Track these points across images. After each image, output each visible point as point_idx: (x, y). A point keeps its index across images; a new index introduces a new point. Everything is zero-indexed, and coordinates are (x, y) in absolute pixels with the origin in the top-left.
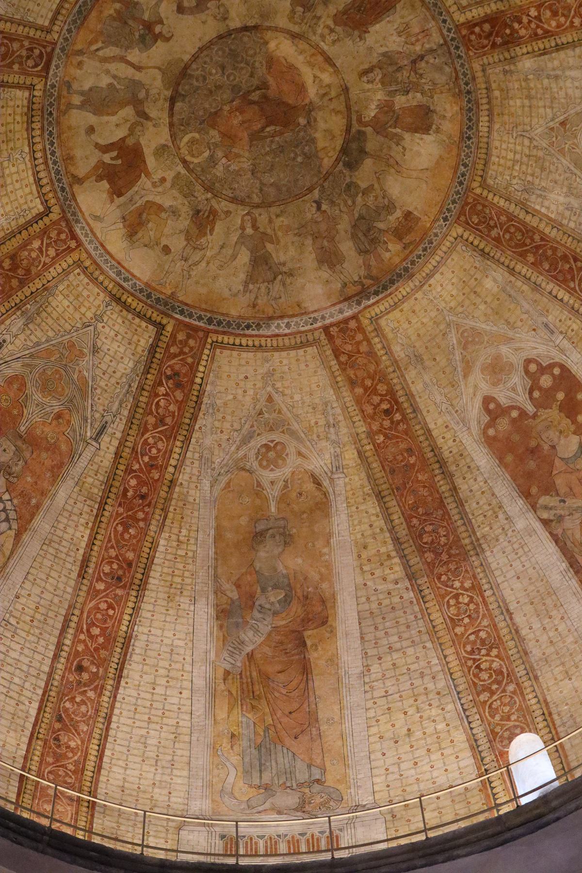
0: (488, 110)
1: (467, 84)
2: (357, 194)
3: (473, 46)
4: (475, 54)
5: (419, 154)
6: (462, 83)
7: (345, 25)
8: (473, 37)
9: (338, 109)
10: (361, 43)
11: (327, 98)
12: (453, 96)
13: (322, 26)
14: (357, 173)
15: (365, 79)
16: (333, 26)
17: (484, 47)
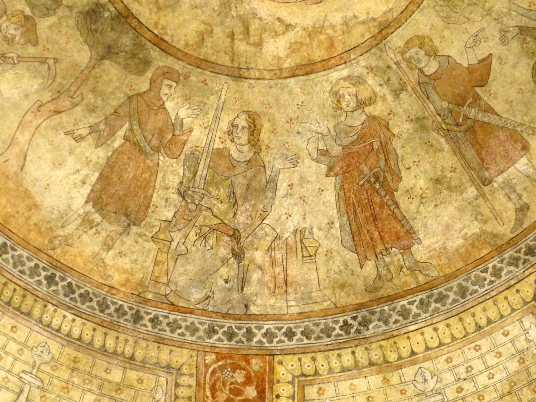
0: (91, 343)
1: (155, 321)
2: (33, 7)
3: (222, 368)
4: (207, 366)
5: (58, 164)
6: (160, 313)
7: (361, 137)
8: (239, 377)
9: (208, 42)
10: (312, 148)
11: (239, 30)
12: (141, 283)
13: (378, 89)
14: (72, 22)
15: (242, 122)
16: (367, 110)
17: (213, 389)
